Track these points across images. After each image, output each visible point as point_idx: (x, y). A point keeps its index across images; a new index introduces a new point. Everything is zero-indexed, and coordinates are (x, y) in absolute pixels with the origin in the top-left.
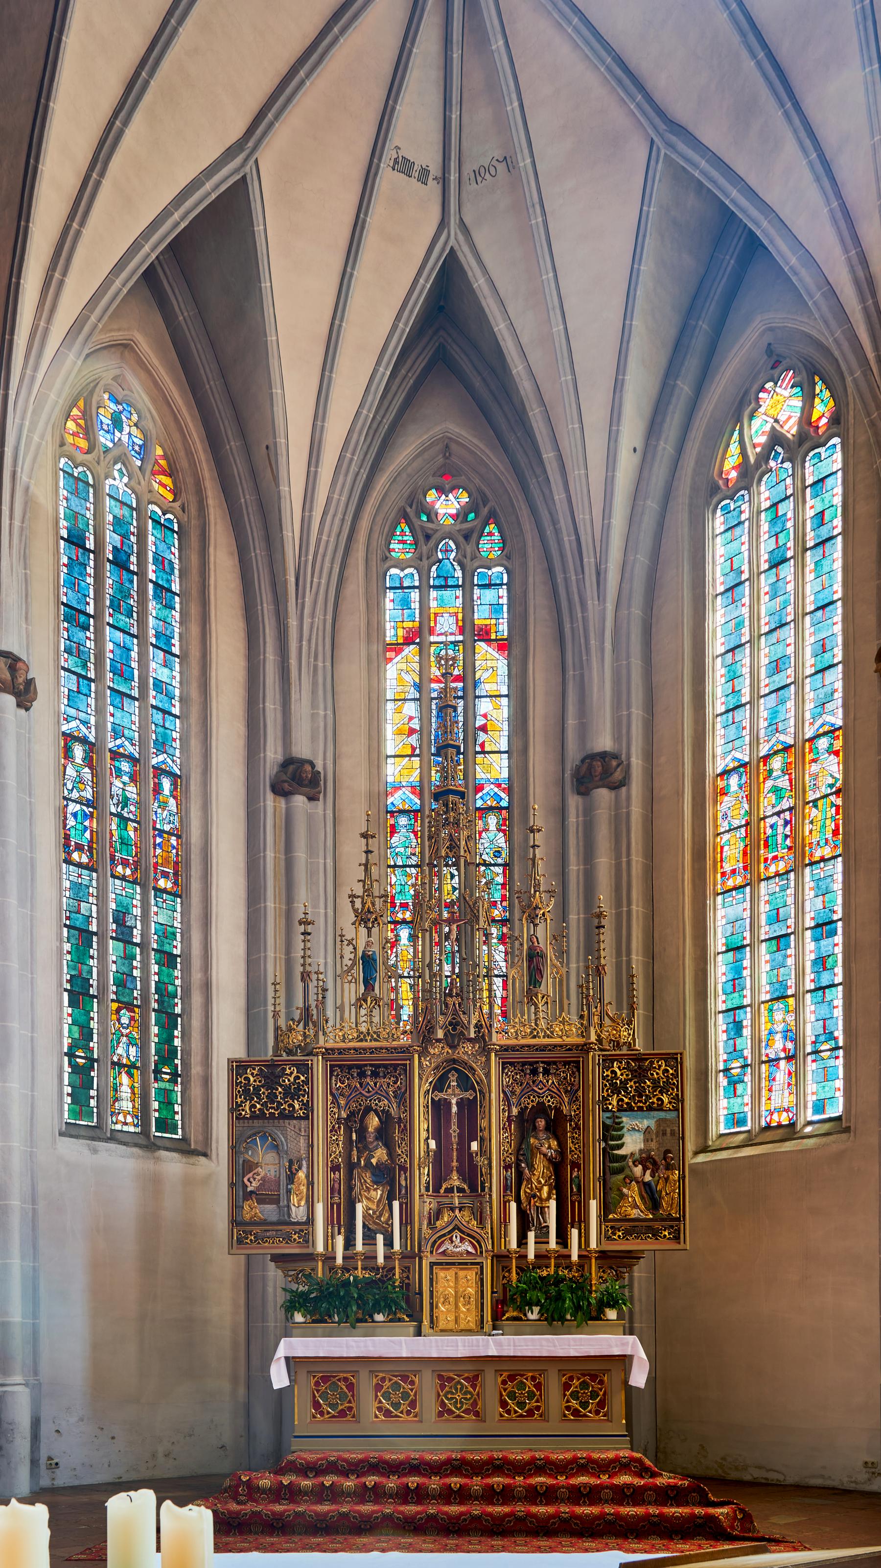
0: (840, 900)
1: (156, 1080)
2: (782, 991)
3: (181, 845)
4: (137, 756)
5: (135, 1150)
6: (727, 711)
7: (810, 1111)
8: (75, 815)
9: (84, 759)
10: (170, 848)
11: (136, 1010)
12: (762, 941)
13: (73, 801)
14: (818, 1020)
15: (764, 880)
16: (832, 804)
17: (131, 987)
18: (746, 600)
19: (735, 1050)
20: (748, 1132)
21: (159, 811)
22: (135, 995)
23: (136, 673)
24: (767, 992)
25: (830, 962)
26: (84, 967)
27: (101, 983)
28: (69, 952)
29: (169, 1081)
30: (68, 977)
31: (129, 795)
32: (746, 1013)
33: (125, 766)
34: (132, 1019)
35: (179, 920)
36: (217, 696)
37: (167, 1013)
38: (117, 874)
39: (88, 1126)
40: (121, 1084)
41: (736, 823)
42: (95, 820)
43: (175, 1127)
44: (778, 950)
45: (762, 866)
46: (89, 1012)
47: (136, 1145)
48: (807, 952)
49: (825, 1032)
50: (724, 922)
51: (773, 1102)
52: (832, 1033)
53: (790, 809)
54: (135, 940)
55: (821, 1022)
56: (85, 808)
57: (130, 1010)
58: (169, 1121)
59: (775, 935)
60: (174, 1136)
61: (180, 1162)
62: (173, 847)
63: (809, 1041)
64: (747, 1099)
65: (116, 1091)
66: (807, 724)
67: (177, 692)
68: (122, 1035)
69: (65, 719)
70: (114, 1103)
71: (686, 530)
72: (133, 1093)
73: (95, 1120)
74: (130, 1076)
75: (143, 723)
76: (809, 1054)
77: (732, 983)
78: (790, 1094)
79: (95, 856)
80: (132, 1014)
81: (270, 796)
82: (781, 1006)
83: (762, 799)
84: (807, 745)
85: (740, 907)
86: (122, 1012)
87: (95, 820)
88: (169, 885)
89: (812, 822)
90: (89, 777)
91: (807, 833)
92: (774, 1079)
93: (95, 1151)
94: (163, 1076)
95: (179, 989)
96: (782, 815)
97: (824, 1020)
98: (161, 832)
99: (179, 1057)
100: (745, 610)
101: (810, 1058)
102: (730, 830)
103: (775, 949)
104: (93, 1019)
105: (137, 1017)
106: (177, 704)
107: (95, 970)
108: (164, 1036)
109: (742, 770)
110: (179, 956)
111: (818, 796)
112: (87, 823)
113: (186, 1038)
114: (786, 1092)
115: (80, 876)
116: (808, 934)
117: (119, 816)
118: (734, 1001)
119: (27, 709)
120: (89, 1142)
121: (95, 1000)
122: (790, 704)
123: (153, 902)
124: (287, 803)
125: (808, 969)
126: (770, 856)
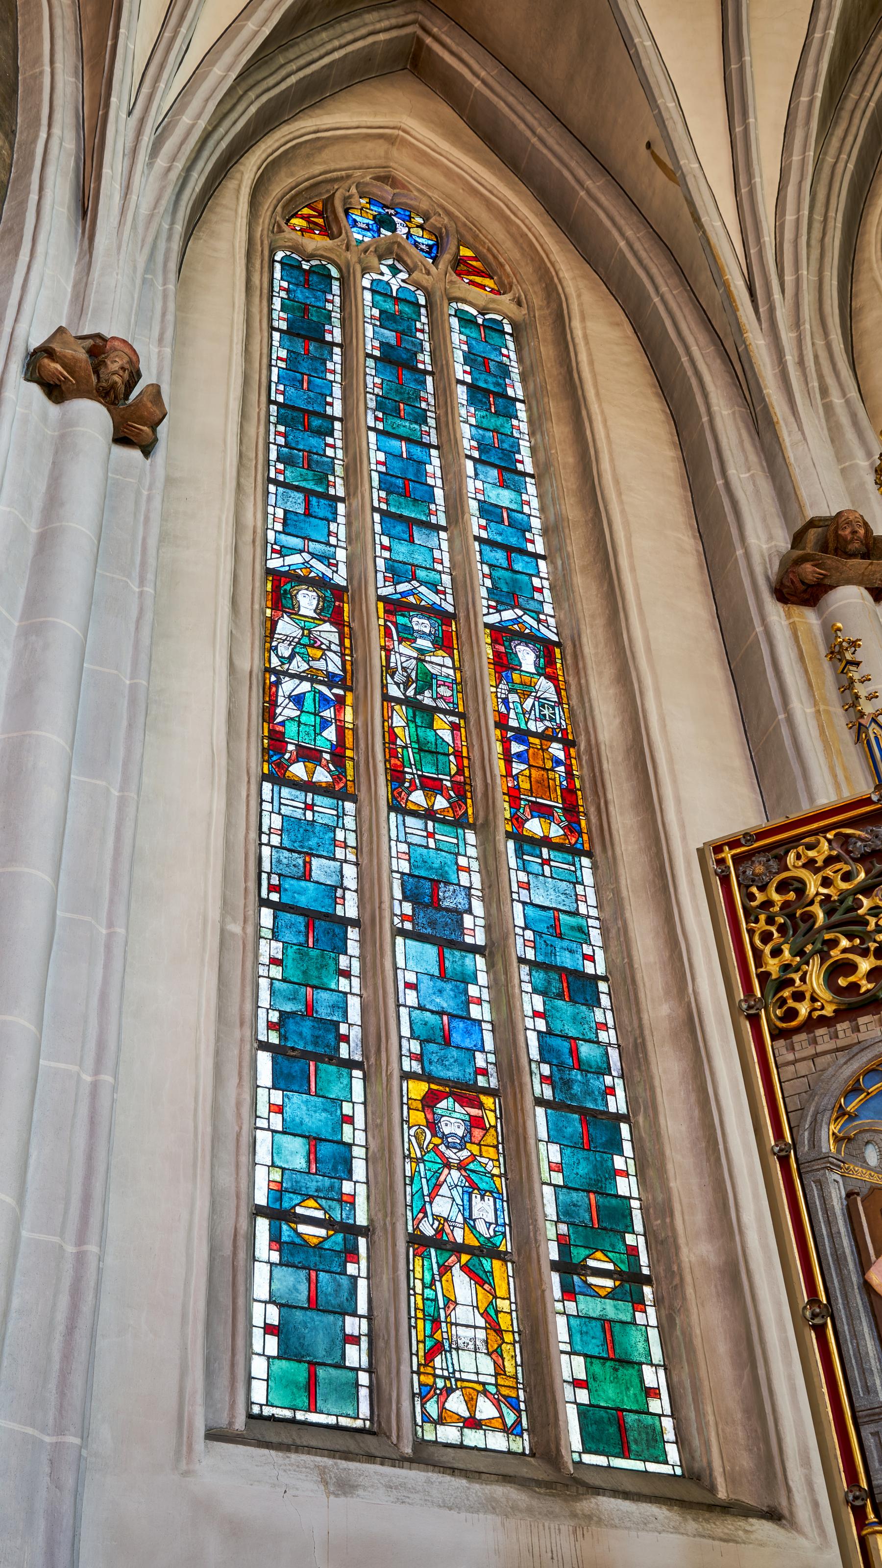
1: (569, 1293)
3: (579, 757)
4: (451, 609)
5: (500, 1491)
8: (298, 700)
9: (319, 611)
10: (549, 765)
11: (488, 1101)
13: (293, 676)
17: (468, 1043)
21: (513, 697)
22: (480, 1062)
23: (439, 494)
26: (323, 995)
27: (372, 1030)
28: (274, 961)
29: (612, 1295)
30: (274, 1017)
31: (434, 670)
33: (421, 624)
34: (476, 1123)
35: (592, 900)
36: (619, 494)
37: (583, 1112)
38: (410, 806)
39: (337, 1427)
40: (451, 1303)
42: (349, 711)
43: (655, 1438)
46: (338, 1102)
47: (506, 1479)
54: (469, 940)
56: (324, 689)
57: (463, 1101)
58: (630, 1418)
60: (652, 1467)
61: (676, 1530)
62: (558, 762)
65: (436, 1323)
67: (536, 523)
68: (447, 1165)
69: (274, 551)
70: (430, 1356)
72: (493, 1326)
73: (364, 1409)
74: (479, 1279)
75: (459, 558)
79: (350, 771)
80: (474, 1112)
81: (776, 613)
86: (443, 1104)
87: (349, 711)
88: (556, 832)
90: (335, 638)
93: (345, 1487)
94: (592, 1280)
95: (614, 1054)
98: (522, 735)
99: (638, 1227)
104: (350, 1120)
105: (491, 1118)
106: (539, 540)
107: (354, 1005)
108: (583, 1169)
110: (605, 979)
112: (329, 713)
113: (651, 1173)
115: (309, 807)
117: (413, 704)
119: (147, 450)
120: (328, 1462)
121: (357, 1073)
123: (513, 863)
124: (820, 614)
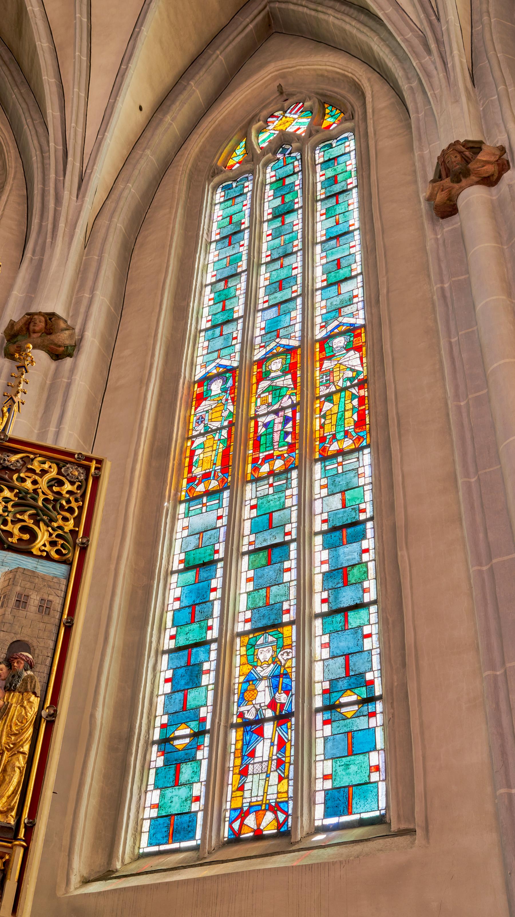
0: (368, 496)
2: (273, 617)
6: (214, 327)
7: (319, 810)
12: (244, 554)
14: (333, 657)
15: (251, 481)
16: (353, 395)
18: (246, 242)
19: (184, 708)
20: (196, 848)
24: (246, 621)
25: (354, 575)
32: (209, 651)
41: (215, 425)
44: (269, 563)
45: (250, 467)
48: (317, 563)
49: (347, 674)
50: (185, 533)
51: (247, 794)
52: (362, 675)
53: (293, 406)
55: (341, 661)
59: (265, 544)
63: (318, 689)
64: (198, 790)
66: (317, 328)
71: (184, 188)
76: (318, 710)
77: (190, 610)
78: (280, 779)
82: (270, 639)
83: (254, 399)
84: (318, 345)
85: (213, 516)
89: (324, 416)
91: (318, 428)
92: (252, 754)
96: (281, 414)
97: (347, 656)
100: (244, 250)
101: (319, 718)
102: (206, 432)
103: (264, 562)
109: (228, 375)
111: (333, 389)
114: (274, 777)
116: (318, 540)
118: (190, 635)
122: (297, 314)
125: (318, 585)
126: (262, 455)
